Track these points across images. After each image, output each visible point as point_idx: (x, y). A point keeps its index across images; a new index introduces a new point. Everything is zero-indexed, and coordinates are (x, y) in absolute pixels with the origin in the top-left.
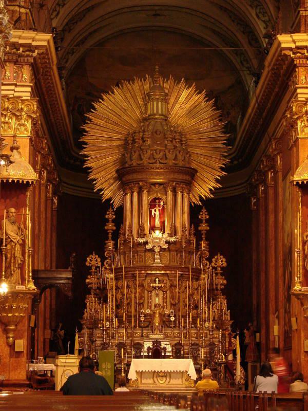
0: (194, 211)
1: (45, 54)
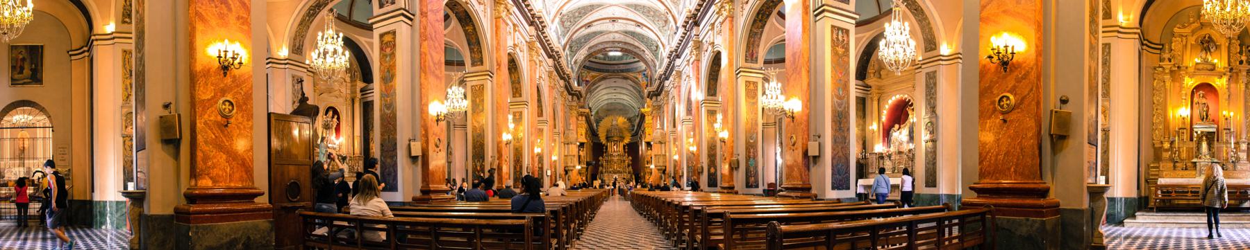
0: (624, 146)
1: (588, 113)
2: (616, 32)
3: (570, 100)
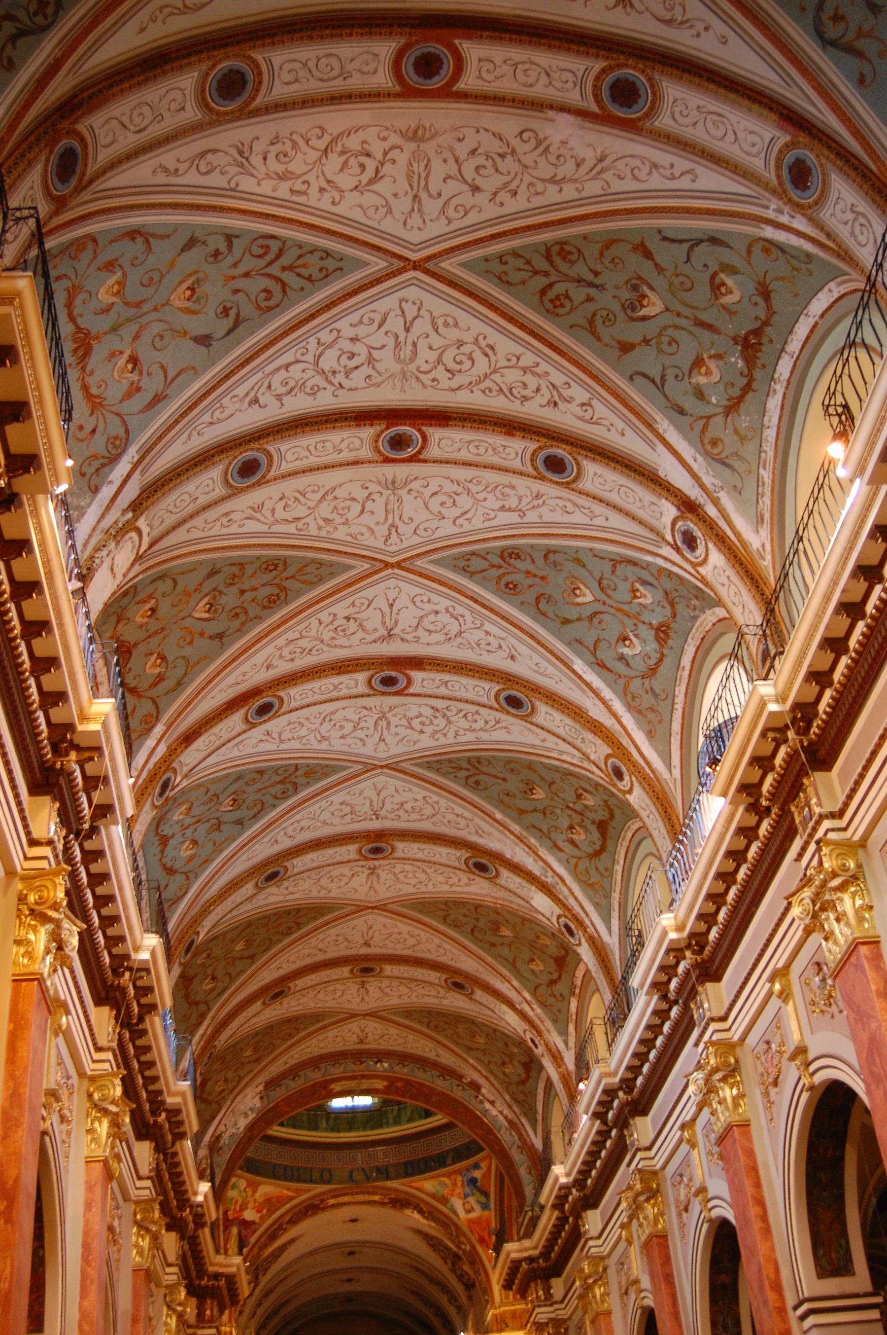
2: (373, 1015)
3: (192, 1320)
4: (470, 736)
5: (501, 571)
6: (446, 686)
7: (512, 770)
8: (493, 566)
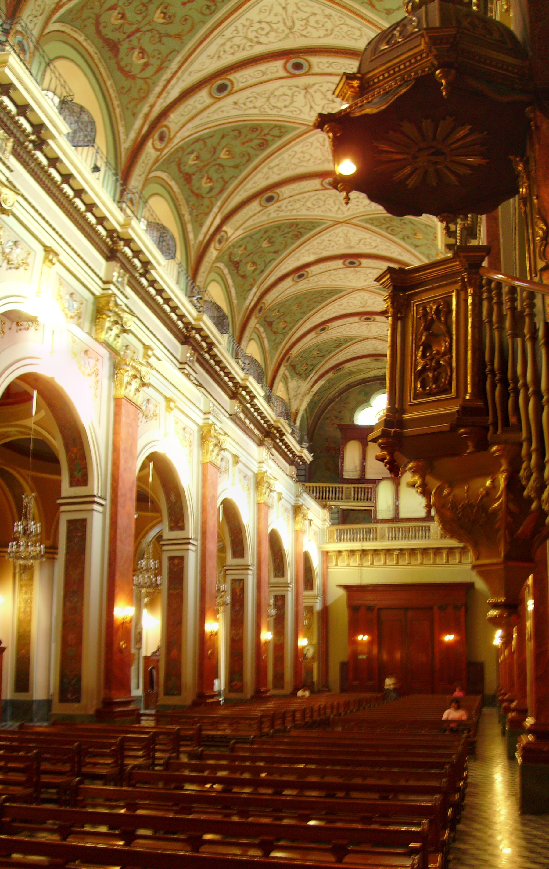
4: (228, 33)
5: (263, 134)
6: (262, 72)
7: (186, 20)
8: (268, 134)
